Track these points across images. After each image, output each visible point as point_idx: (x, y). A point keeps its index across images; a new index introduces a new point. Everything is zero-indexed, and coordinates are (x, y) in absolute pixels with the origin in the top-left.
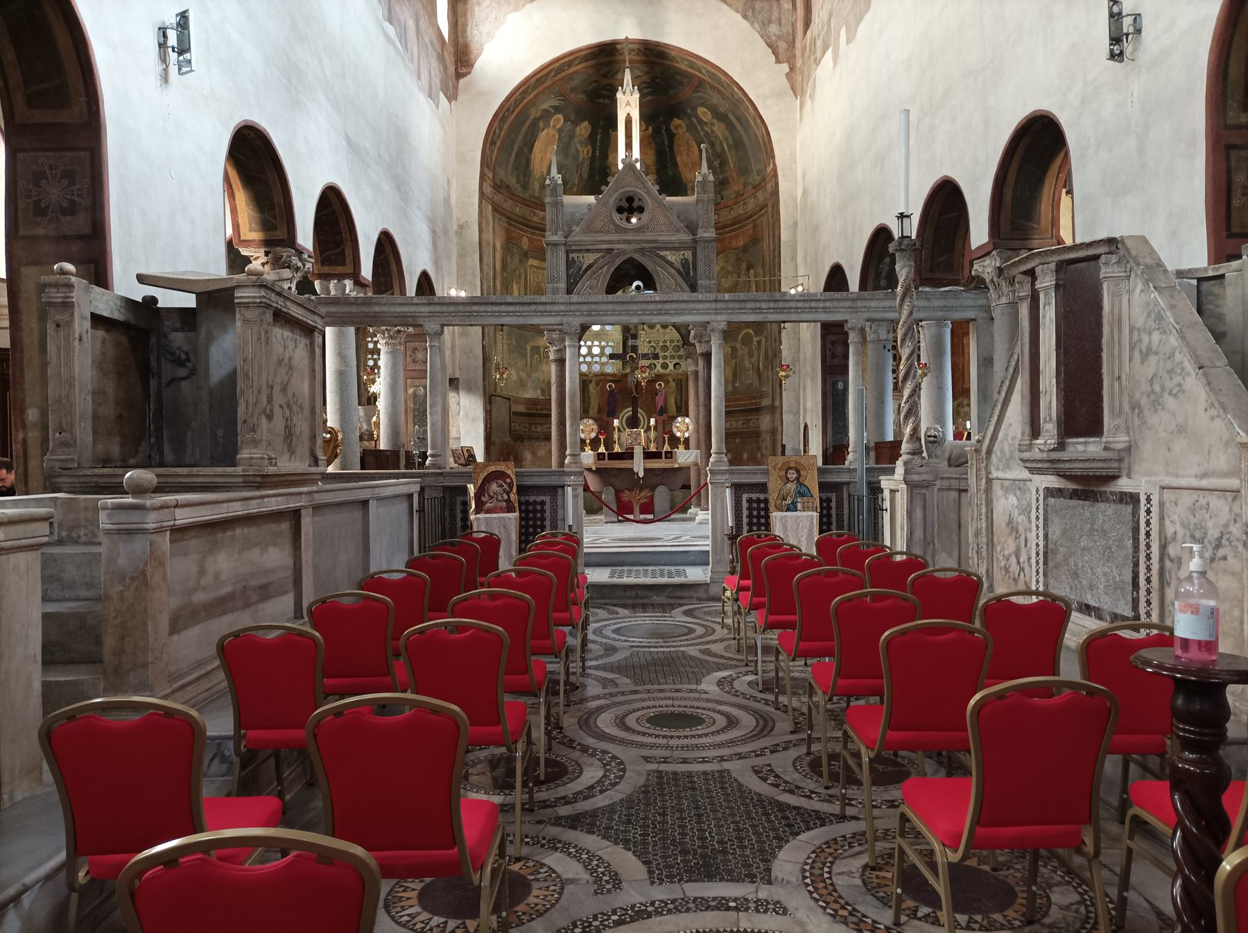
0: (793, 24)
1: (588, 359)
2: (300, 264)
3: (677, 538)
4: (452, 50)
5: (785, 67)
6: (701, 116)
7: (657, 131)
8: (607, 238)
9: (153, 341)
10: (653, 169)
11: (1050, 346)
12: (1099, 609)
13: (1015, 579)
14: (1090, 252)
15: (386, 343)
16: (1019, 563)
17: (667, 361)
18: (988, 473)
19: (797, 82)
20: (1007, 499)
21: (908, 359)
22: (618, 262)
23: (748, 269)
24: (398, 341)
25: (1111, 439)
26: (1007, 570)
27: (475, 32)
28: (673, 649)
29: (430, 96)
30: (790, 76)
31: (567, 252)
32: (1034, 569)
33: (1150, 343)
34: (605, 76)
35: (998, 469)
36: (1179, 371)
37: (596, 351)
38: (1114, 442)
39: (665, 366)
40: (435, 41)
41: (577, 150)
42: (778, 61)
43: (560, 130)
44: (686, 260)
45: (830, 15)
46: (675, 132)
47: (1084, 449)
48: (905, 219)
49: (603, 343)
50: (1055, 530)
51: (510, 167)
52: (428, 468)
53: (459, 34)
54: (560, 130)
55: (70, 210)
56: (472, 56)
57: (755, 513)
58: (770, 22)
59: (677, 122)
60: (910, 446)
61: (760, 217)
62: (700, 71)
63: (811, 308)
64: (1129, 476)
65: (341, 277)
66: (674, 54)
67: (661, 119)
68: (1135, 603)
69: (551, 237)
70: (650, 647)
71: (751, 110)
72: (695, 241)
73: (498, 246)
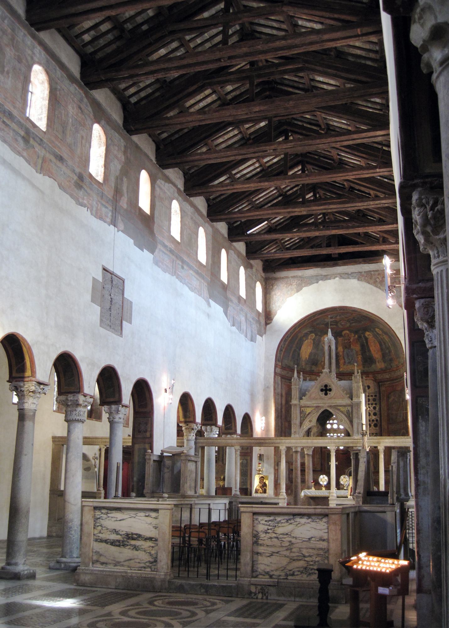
2: (197, 428)
4: (264, 314)
9: (162, 463)
10: (360, 353)
27: (274, 306)
29: (252, 340)
31: (301, 407)
43: (314, 340)
44: (348, 410)
46: (368, 337)
51: (290, 358)
54: (314, 340)
56: (272, 316)
59: (367, 334)
65: (211, 425)
67: (361, 332)
73: (284, 394)
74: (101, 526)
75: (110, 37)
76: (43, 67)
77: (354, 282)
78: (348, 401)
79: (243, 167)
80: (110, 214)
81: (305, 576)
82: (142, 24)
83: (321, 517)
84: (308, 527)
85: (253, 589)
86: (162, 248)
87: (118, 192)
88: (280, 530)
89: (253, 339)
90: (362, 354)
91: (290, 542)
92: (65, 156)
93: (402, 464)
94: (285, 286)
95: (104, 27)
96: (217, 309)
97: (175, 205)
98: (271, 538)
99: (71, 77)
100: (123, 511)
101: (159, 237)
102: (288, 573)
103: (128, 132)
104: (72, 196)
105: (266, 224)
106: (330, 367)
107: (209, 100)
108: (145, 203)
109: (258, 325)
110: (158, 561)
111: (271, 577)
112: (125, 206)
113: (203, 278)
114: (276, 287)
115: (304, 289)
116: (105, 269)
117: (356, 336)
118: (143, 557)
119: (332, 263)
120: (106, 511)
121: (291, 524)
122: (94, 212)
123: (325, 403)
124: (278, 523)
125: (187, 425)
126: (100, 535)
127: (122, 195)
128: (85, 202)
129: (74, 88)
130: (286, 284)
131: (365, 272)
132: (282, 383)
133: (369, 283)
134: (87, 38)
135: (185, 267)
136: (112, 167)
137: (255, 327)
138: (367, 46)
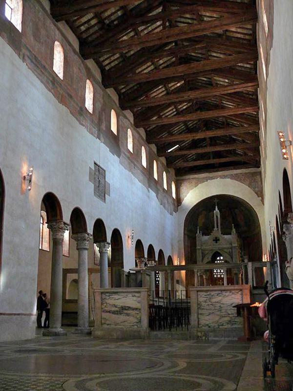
1: (217, 274)
5: (260, 198)
22: (213, 253)
29: (171, 214)
55: (119, 260)
58: (256, 188)
59: (236, 210)
65: (152, 260)
72: (232, 247)
74: (106, 303)
75: (96, 28)
76: (60, 43)
77: (228, 180)
78: (230, 246)
79: (167, 111)
80: (97, 132)
81: (229, 326)
82: (115, 20)
83: (237, 291)
84: (230, 298)
85: (199, 334)
86: (124, 155)
87: (100, 120)
88: (214, 300)
89: (171, 214)
91: (220, 306)
92: (73, 95)
93: (272, 270)
95: (93, 22)
96: (153, 194)
97: (129, 132)
98: (208, 305)
99: (74, 51)
100: (119, 294)
101: (122, 149)
102: (220, 324)
103: (104, 87)
104: (77, 119)
105: (178, 147)
106: (218, 227)
107: (149, 69)
108: (114, 128)
110: (142, 321)
111: (209, 327)
112: (104, 129)
113: (145, 176)
114: (183, 184)
116: (95, 163)
118: (133, 320)
120: (109, 294)
121: (220, 296)
122: (89, 130)
123: (216, 247)
124: (212, 296)
126: (106, 308)
127: (102, 122)
128: (84, 124)
129: (76, 57)
134: (83, 28)
135: (136, 168)
136: (97, 105)
137: (172, 207)
138: (245, 31)
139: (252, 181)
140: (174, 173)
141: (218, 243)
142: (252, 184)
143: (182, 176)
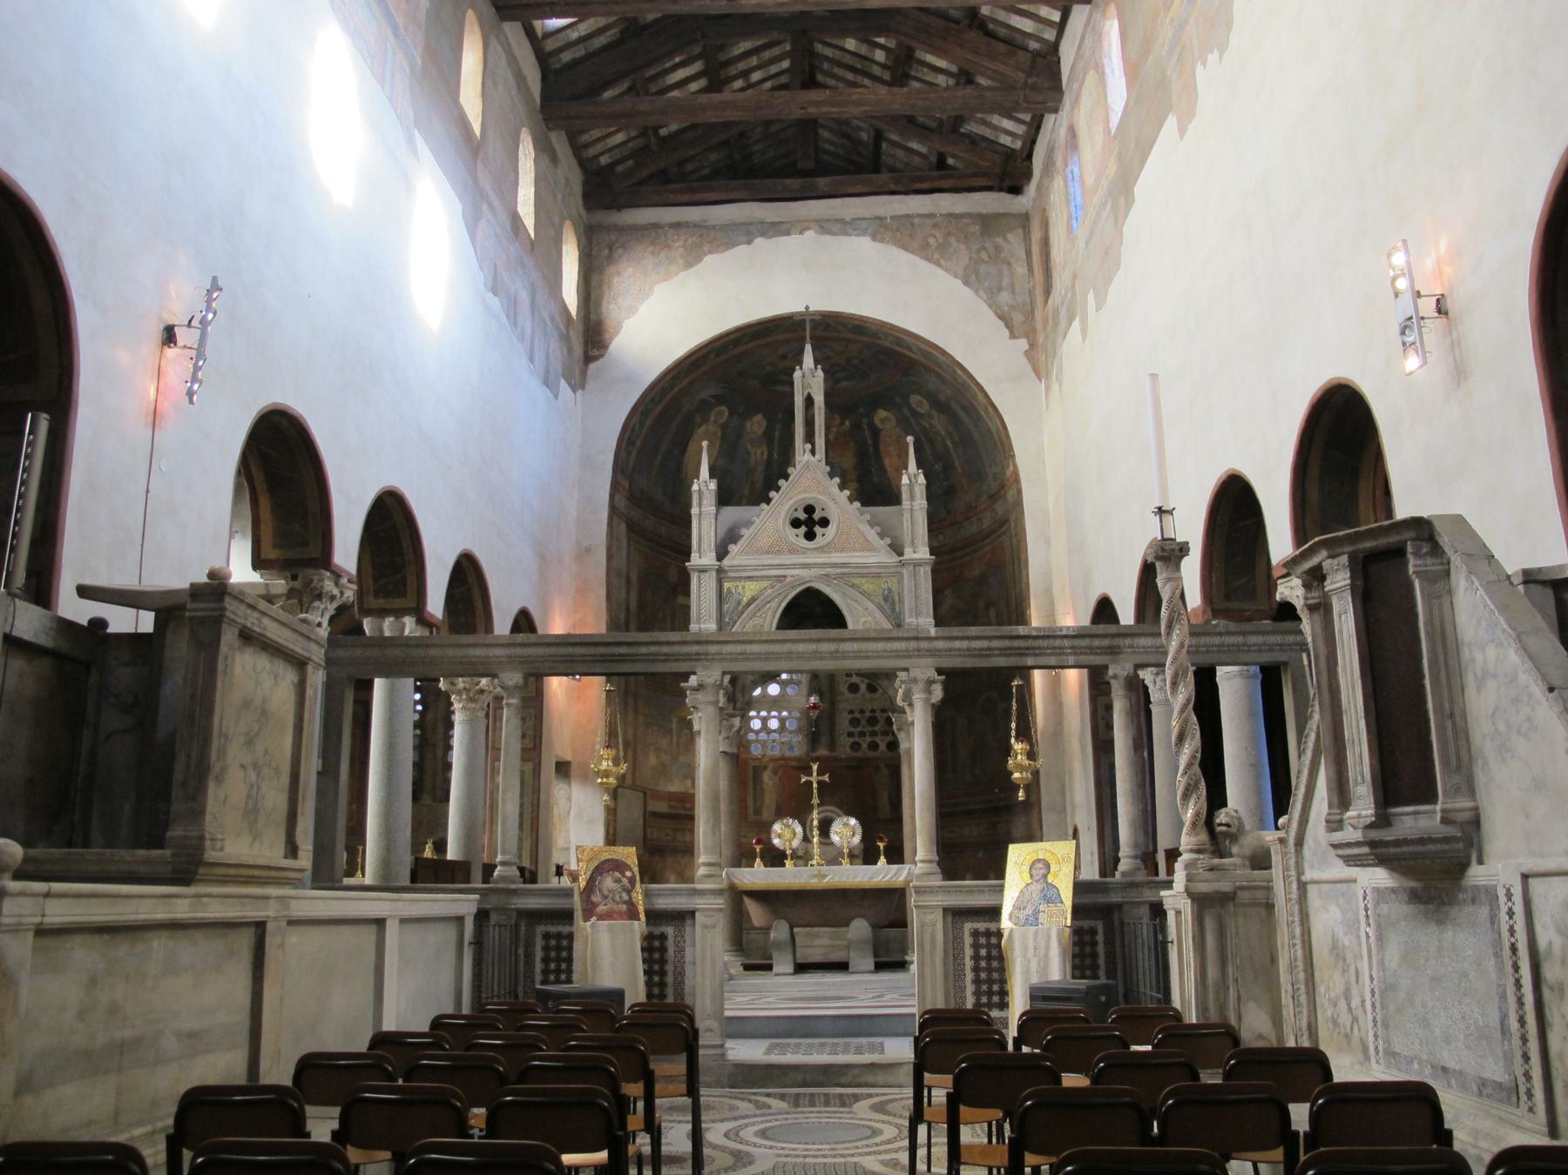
0: (1030, 291)
1: (763, 736)
2: (336, 592)
3: (879, 997)
4: (580, 328)
5: (1023, 344)
6: (914, 406)
7: (857, 426)
8: (778, 562)
9: (94, 677)
11: (1352, 676)
12: (1461, 1073)
13: (1347, 1036)
14: (1393, 539)
15: (464, 708)
16: (1350, 1009)
17: (878, 739)
18: (1300, 873)
19: (1040, 359)
20: (1327, 911)
21: (1182, 711)
23: (988, 607)
24: (479, 704)
25: (1449, 806)
26: (1335, 1023)
27: (612, 307)
28: (842, 1160)
29: (546, 383)
30: (1032, 354)
31: (720, 582)
32: (1370, 1017)
33: (1485, 661)
34: (784, 357)
35: (1312, 867)
36: (1526, 699)
37: (774, 724)
38: (1454, 810)
39: (874, 746)
40: (557, 317)
41: (748, 453)
42: (1013, 336)
43: (724, 427)
44: (889, 589)
45: (1074, 277)
47: (1414, 821)
48: (1163, 515)
49: (785, 714)
50: (1393, 952)
52: (496, 882)
53: (592, 309)
54: (724, 427)
56: (607, 336)
57: (983, 952)
58: (1000, 289)
60: (1193, 839)
61: (999, 537)
62: (909, 348)
63: (1054, 648)
64: (1480, 862)
65: (399, 613)
66: (873, 328)
68: (1508, 1057)
69: (696, 560)
70: (805, 1157)
71: (980, 397)
72: (902, 564)
73: (634, 577)
77: (862, 245)
89: (547, 382)
90: (859, 481)
94: (651, 249)
109: (565, 352)
114: (620, 251)
115: (708, 259)
117: (847, 423)
119: (794, 183)
125: (294, 578)
130: (653, 243)
131: (892, 218)
132: (629, 546)
133: (906, 250)
139: (984, 256)
140: (577, 188)
141: (819, 541)
142: (983, 268)
143: (619, 208)
